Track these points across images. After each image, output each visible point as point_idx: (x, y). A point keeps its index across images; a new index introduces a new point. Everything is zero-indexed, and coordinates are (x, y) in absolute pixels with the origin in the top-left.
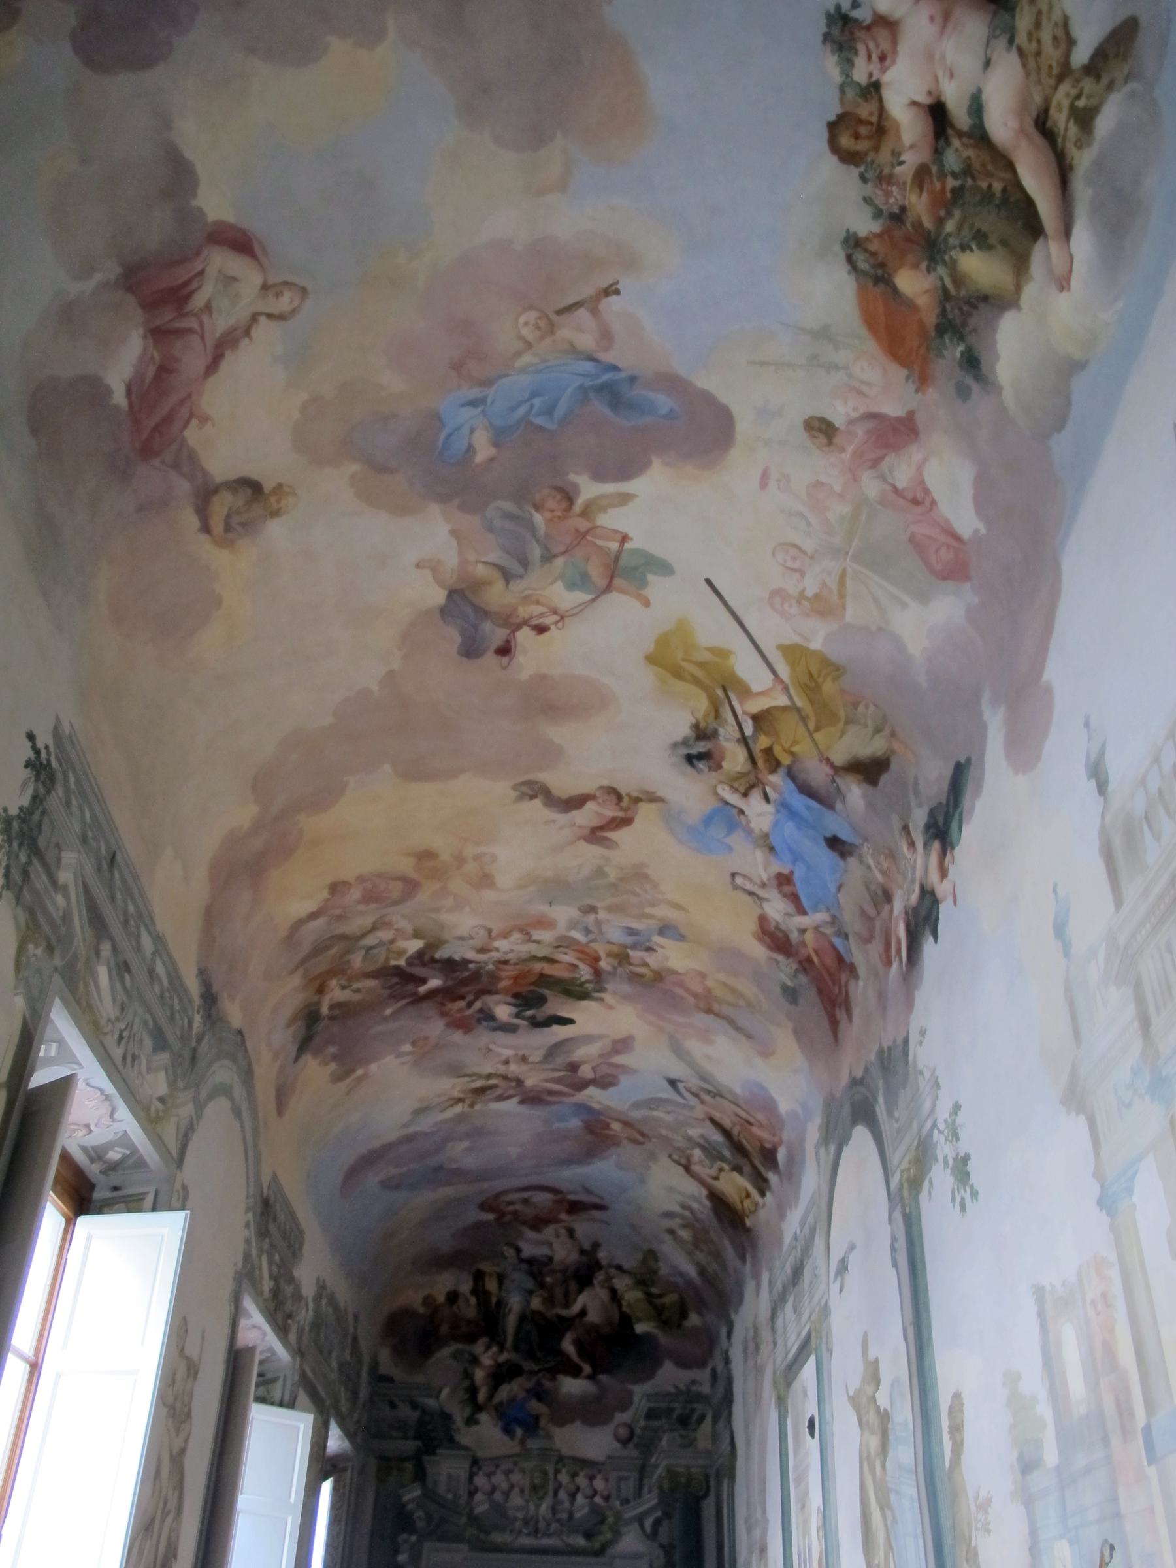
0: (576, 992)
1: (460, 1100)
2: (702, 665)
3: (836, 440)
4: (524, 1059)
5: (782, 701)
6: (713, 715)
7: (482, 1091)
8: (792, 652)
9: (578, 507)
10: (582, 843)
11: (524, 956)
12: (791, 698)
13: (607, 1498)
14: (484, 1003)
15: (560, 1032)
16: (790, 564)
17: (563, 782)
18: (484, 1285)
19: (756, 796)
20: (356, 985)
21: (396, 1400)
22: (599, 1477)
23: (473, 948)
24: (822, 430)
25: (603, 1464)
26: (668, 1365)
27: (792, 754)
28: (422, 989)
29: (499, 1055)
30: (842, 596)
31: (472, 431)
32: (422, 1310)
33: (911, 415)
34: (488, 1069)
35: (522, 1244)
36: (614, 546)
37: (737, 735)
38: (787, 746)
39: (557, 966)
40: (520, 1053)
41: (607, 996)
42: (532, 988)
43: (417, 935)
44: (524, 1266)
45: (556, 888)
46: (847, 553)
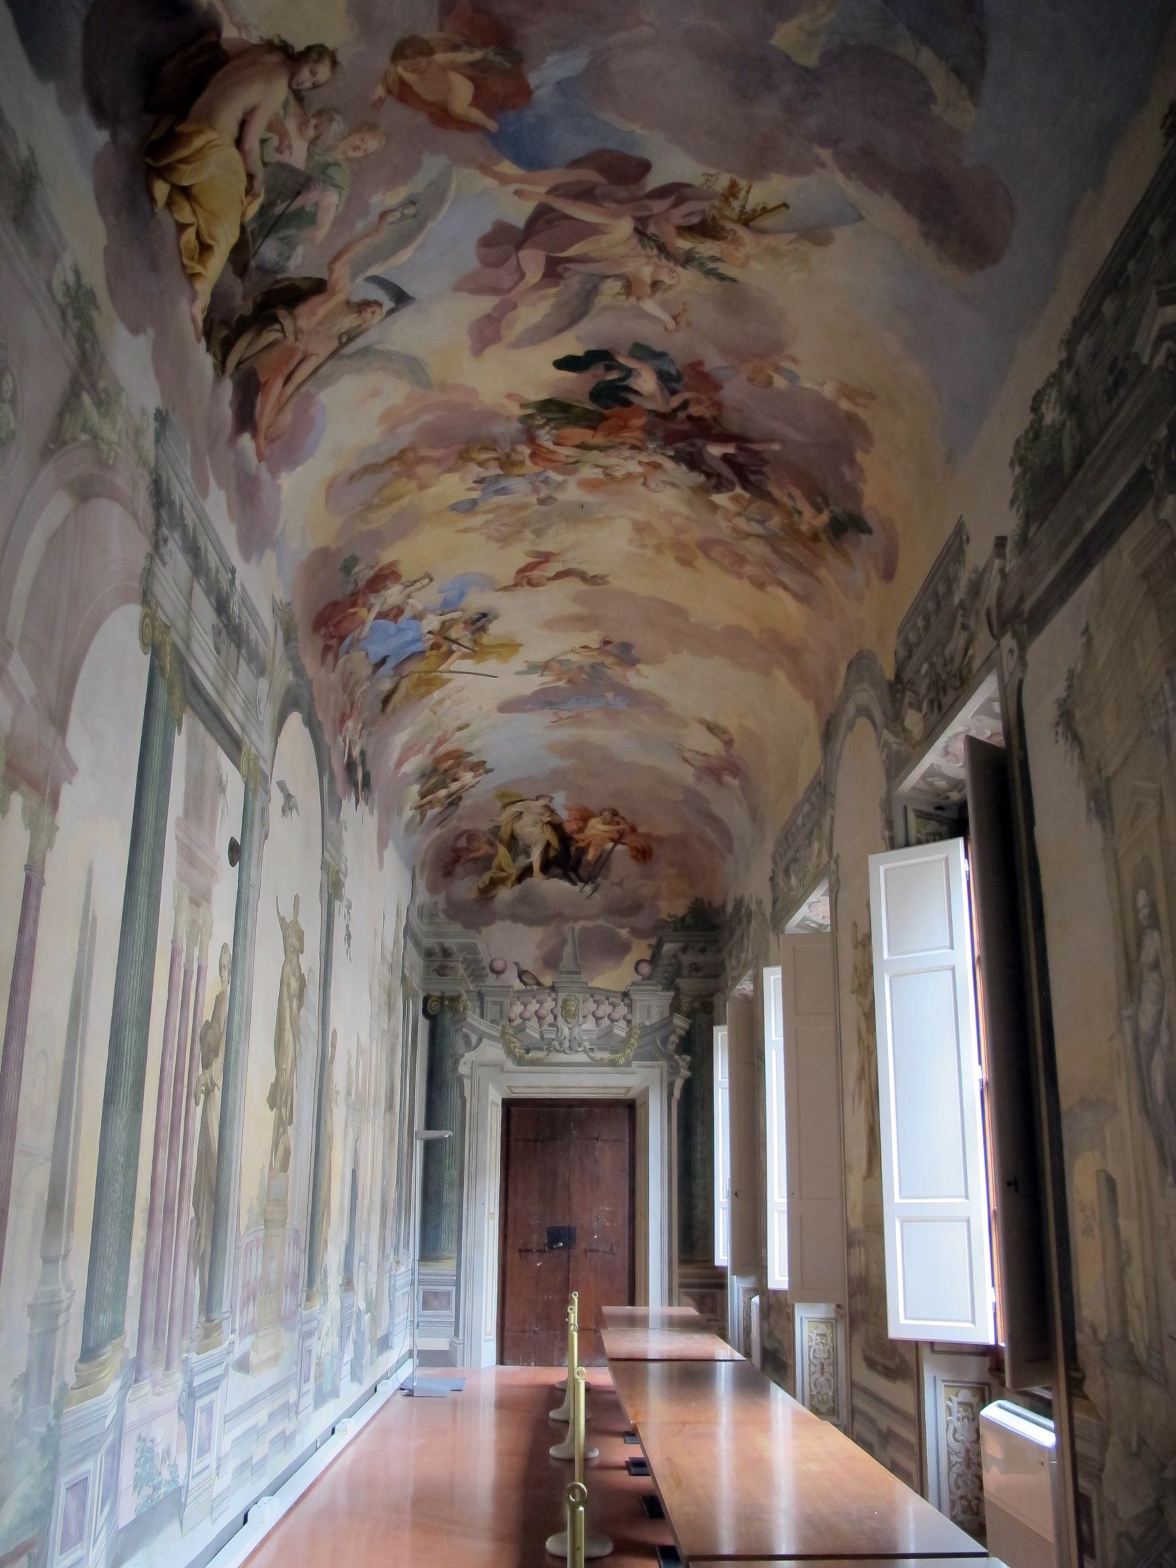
0: (555, 409)
1: (747, 220)
4: (629, 287)
5: (442, 668)
7: (707, 229)
10: (556, 551)
11: (613, 452)
14: (667, 401)
17: (573, 585)
23: (665, 471)
28: (730, 449)
29: (663, 305)
34: (685, 279)
39: (578, 441)
40: (633, 299)
41: (518, 412)
42: (607, 412)
43: (715, 507)
45: (578, 515)
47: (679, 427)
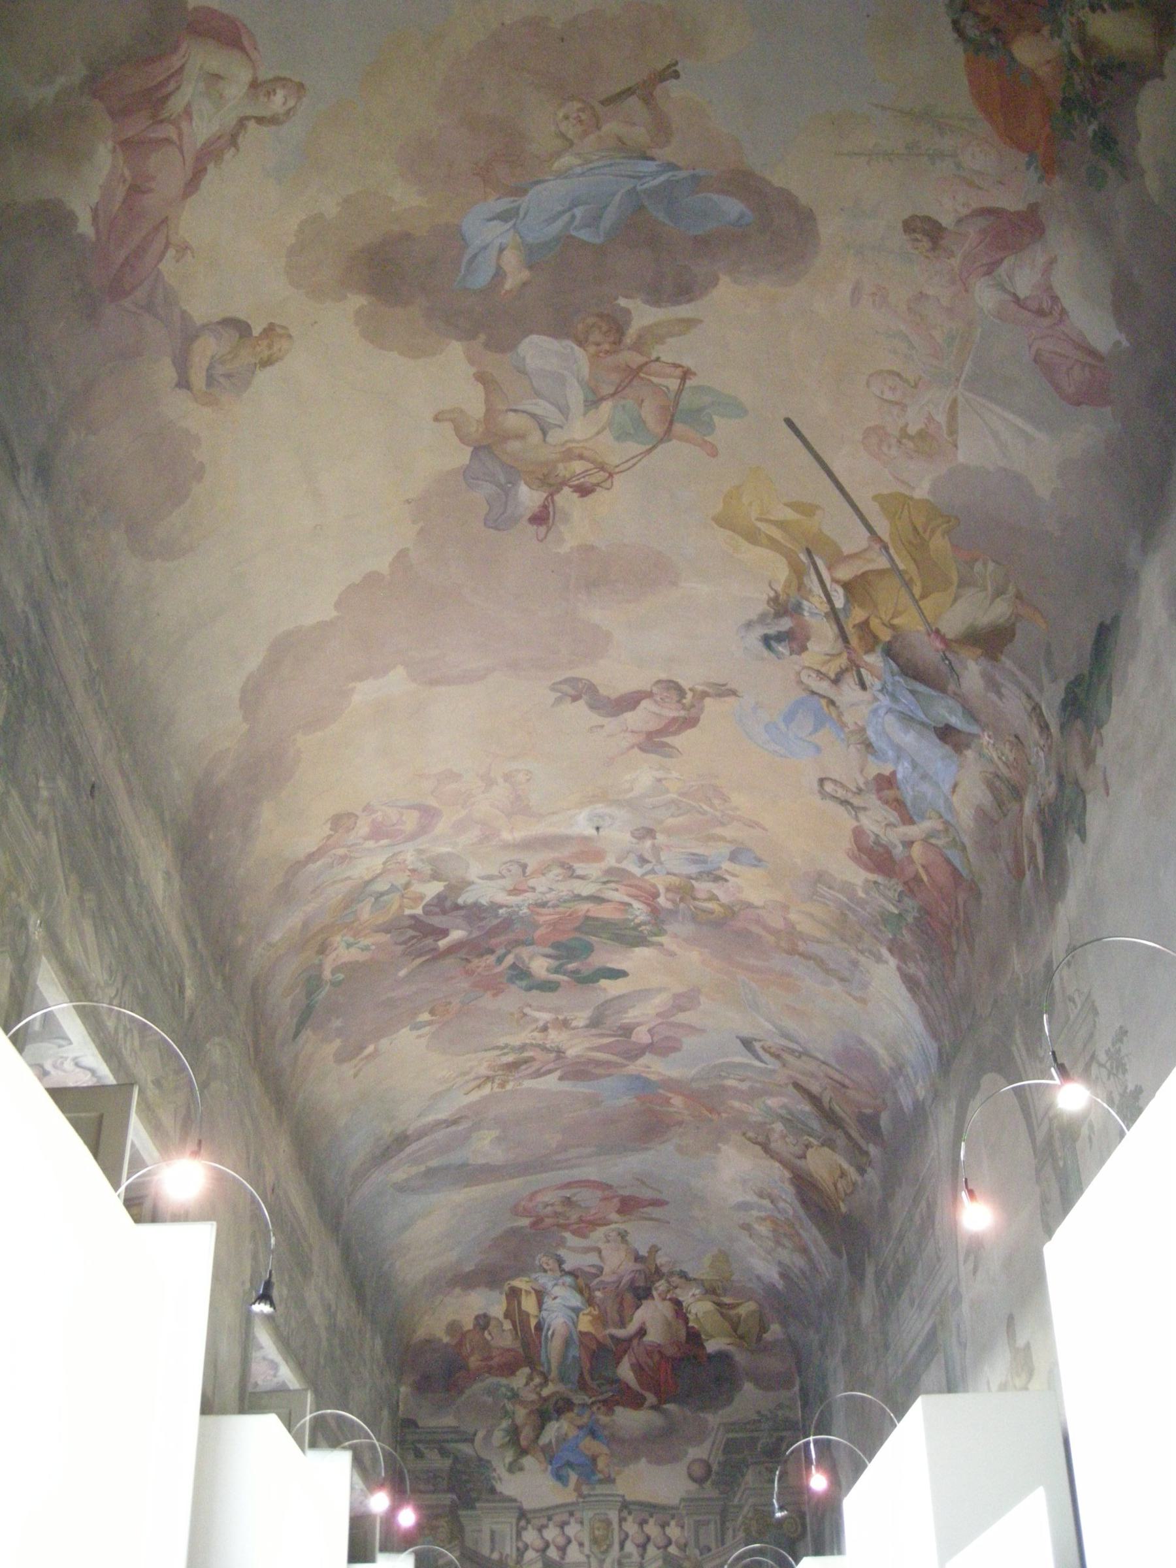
0: (628, 936)
2: (781, 525)
3: (943, 243)
4: (565, 1024)
5: (882, 563)
6: (795, 583)
8: (893, 504)
9: (628, 341)
10: (636, 750)
12: (891, 559)
13: (683, 1547)
14: (517, 957)
15: (612, 988)
16: (888, 395)
18: (519, 1303)
19: (850, 683)
20: (365, 942)
21: (420, 1446)
22: (673, 1523)
23: (504, 889)
24: (927, 231)
25: (677, 1508)
26: (748, 1386)
27: (893, 627)
28: (443, 943)
29: (536, 1020)
30: (953, 432)
31: (501, 250)
32: (446, 1339)
33: (1033, 208)
35: (562, 1252)
36: (673, 384)
37: (826, 608)
38: (886, 618)
39: (604, 906)
40: (561, 1017)
43: (436, 876)
44: (568, 1280)
46: (958, 380)
47: (503, 938)
